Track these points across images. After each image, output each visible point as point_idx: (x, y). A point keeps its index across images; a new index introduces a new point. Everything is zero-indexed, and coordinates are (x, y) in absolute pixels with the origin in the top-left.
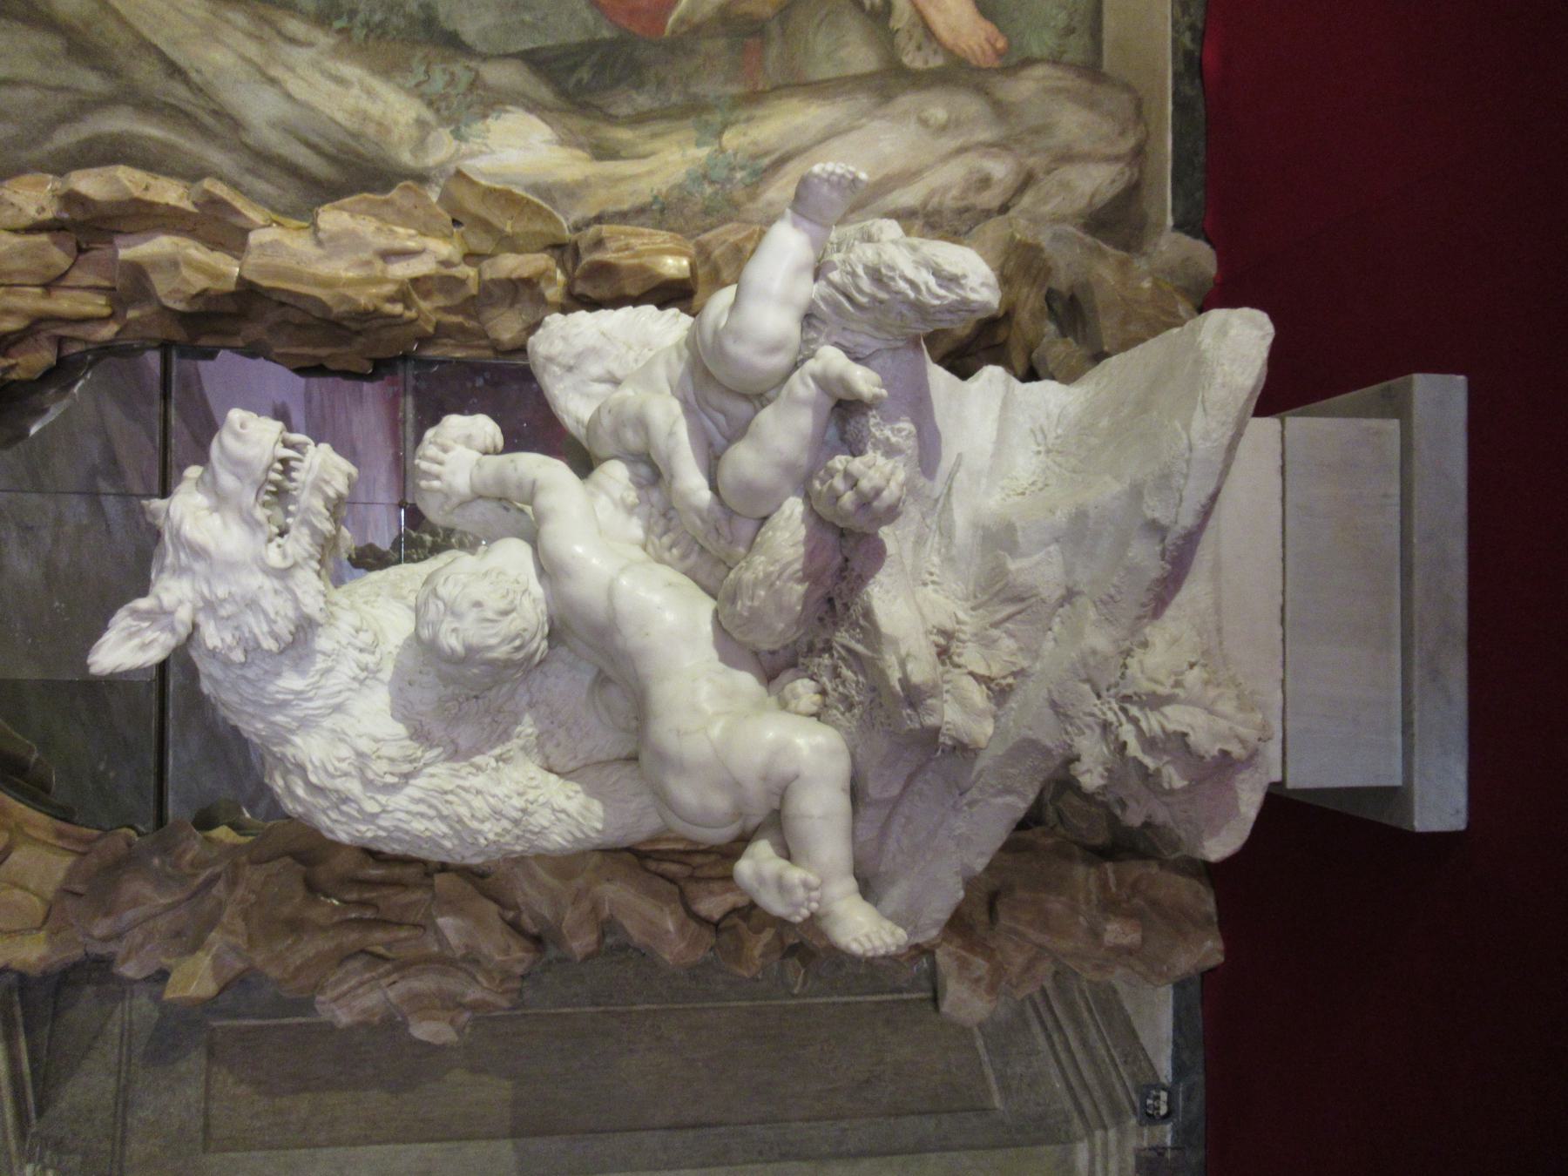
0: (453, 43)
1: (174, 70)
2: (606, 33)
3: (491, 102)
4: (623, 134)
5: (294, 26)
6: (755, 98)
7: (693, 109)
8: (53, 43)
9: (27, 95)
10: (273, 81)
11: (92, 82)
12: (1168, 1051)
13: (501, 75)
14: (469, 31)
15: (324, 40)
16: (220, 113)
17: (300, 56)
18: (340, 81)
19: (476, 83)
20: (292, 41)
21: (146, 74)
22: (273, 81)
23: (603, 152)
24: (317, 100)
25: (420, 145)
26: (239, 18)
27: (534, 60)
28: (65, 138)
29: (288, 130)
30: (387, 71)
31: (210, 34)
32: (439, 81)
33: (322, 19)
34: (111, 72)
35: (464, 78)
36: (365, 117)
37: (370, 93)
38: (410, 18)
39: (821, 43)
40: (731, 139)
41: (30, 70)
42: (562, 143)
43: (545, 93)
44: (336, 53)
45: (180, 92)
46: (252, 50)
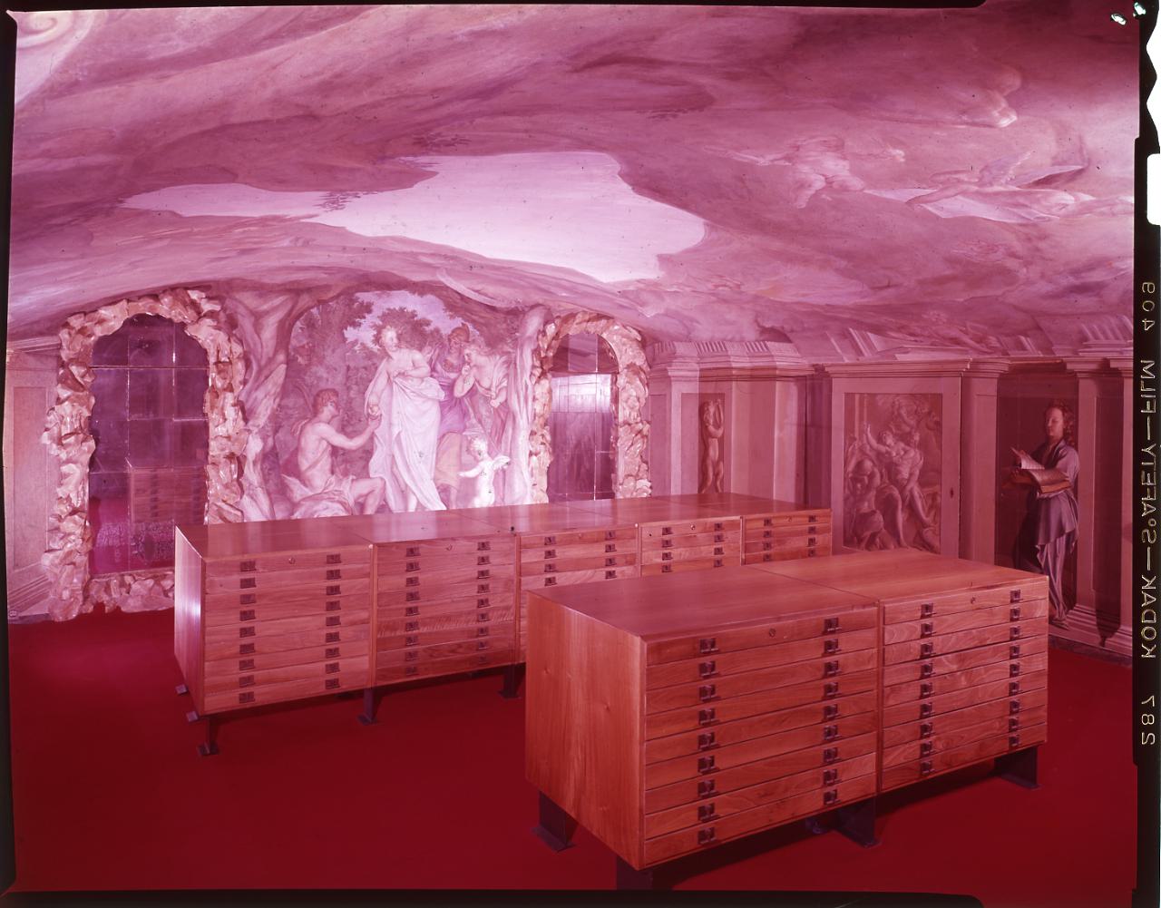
0: (276, 431)
1: (267, 377)
2: (281, 462)
3: (264, 439)
4: (259, 467)
5: (278, 400)
6: (269, 494)
7: (265, 480)
8: (271, 355)
9: (260, 350)
10: (266, 396)
11: (263, 363)
12: (29, 614)
13: (270, 442)
14: (279, 435)
15: (275, 407)
16: (258, 386)
17: (272, 401)
18: (267, 410)
19: (268, 436)
20: (274, 400)
21: (266, 372)
22: (266, 396)
23: (255, 463)
24: (262, 405)
25: (254, 426)
26: (279, 390)
27: (274, 447)
28: (252, 357)
29: (256, 398)
30: (270, 418)
31: (275, 384)
32: (269, 429)
33: (279, 405)
34: (266, 365)
35: (269, 434)
36: (260, 414)
37: (264, 415)
38: (281, 423)
39: (282, 507)
40: (259, 490)
41: (265, 350)
42: (256, 455)
43: (268, 449)
44: (273, 409)
45: (262, 378)
46: (273, 392)
